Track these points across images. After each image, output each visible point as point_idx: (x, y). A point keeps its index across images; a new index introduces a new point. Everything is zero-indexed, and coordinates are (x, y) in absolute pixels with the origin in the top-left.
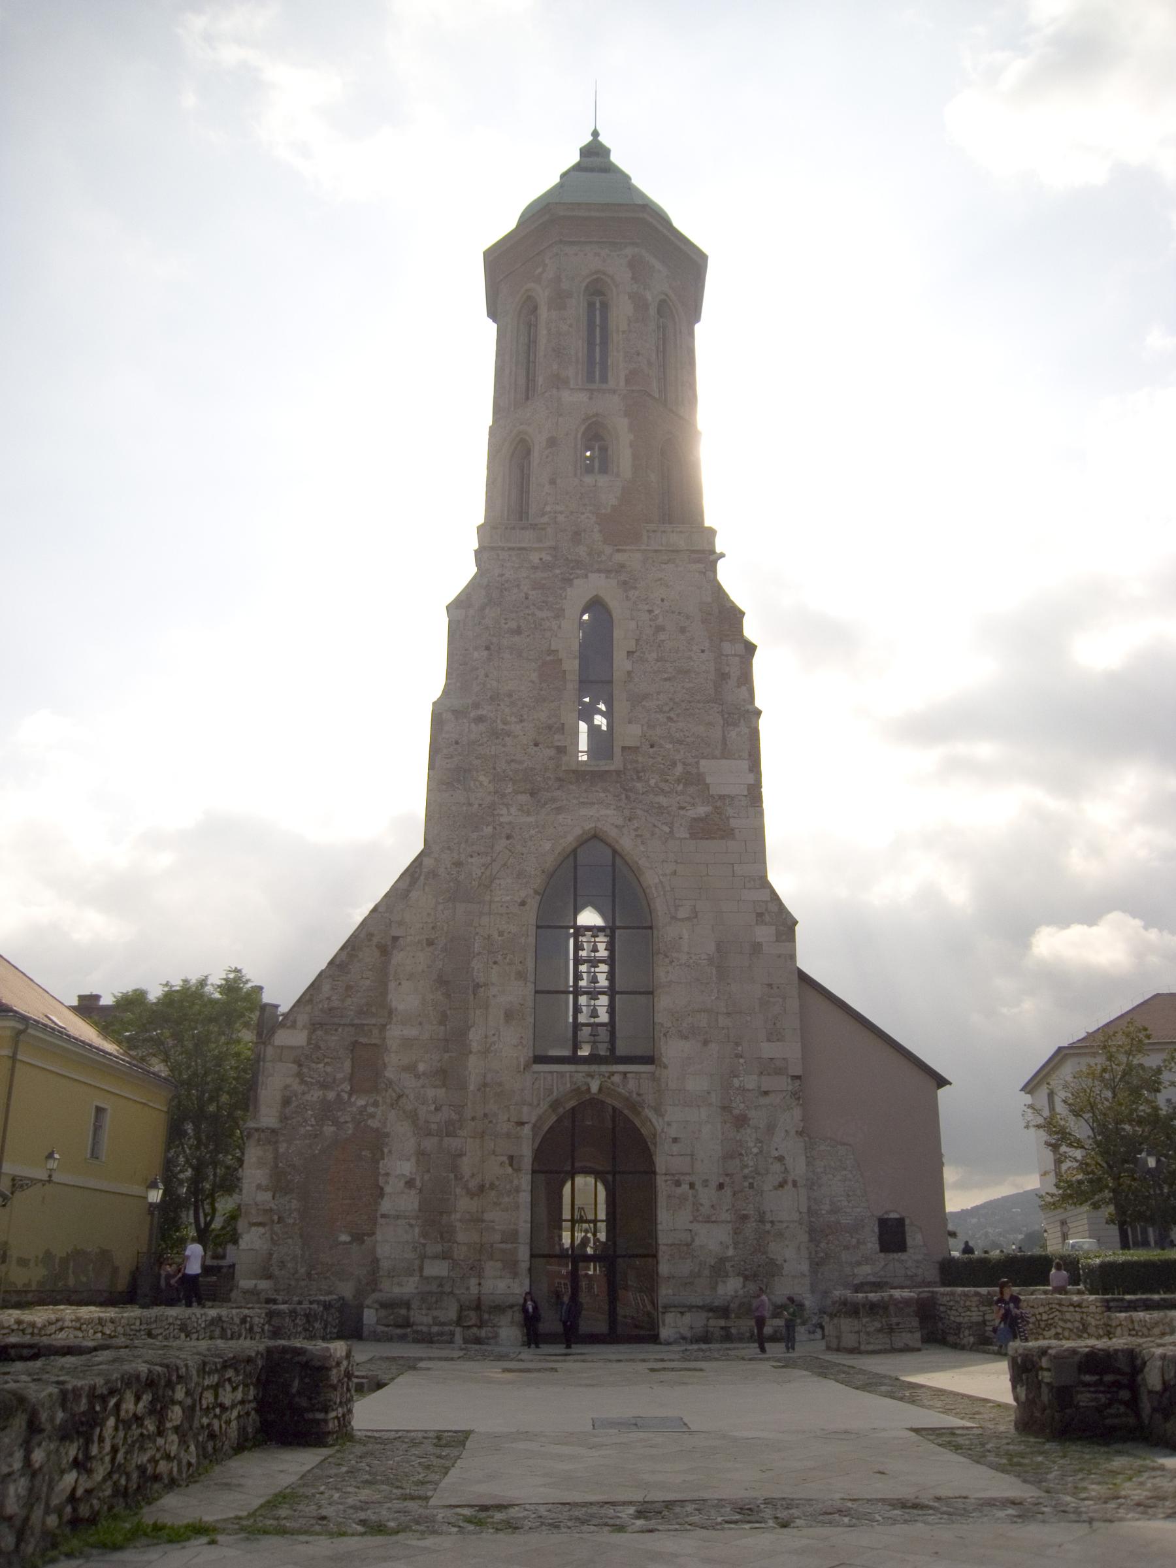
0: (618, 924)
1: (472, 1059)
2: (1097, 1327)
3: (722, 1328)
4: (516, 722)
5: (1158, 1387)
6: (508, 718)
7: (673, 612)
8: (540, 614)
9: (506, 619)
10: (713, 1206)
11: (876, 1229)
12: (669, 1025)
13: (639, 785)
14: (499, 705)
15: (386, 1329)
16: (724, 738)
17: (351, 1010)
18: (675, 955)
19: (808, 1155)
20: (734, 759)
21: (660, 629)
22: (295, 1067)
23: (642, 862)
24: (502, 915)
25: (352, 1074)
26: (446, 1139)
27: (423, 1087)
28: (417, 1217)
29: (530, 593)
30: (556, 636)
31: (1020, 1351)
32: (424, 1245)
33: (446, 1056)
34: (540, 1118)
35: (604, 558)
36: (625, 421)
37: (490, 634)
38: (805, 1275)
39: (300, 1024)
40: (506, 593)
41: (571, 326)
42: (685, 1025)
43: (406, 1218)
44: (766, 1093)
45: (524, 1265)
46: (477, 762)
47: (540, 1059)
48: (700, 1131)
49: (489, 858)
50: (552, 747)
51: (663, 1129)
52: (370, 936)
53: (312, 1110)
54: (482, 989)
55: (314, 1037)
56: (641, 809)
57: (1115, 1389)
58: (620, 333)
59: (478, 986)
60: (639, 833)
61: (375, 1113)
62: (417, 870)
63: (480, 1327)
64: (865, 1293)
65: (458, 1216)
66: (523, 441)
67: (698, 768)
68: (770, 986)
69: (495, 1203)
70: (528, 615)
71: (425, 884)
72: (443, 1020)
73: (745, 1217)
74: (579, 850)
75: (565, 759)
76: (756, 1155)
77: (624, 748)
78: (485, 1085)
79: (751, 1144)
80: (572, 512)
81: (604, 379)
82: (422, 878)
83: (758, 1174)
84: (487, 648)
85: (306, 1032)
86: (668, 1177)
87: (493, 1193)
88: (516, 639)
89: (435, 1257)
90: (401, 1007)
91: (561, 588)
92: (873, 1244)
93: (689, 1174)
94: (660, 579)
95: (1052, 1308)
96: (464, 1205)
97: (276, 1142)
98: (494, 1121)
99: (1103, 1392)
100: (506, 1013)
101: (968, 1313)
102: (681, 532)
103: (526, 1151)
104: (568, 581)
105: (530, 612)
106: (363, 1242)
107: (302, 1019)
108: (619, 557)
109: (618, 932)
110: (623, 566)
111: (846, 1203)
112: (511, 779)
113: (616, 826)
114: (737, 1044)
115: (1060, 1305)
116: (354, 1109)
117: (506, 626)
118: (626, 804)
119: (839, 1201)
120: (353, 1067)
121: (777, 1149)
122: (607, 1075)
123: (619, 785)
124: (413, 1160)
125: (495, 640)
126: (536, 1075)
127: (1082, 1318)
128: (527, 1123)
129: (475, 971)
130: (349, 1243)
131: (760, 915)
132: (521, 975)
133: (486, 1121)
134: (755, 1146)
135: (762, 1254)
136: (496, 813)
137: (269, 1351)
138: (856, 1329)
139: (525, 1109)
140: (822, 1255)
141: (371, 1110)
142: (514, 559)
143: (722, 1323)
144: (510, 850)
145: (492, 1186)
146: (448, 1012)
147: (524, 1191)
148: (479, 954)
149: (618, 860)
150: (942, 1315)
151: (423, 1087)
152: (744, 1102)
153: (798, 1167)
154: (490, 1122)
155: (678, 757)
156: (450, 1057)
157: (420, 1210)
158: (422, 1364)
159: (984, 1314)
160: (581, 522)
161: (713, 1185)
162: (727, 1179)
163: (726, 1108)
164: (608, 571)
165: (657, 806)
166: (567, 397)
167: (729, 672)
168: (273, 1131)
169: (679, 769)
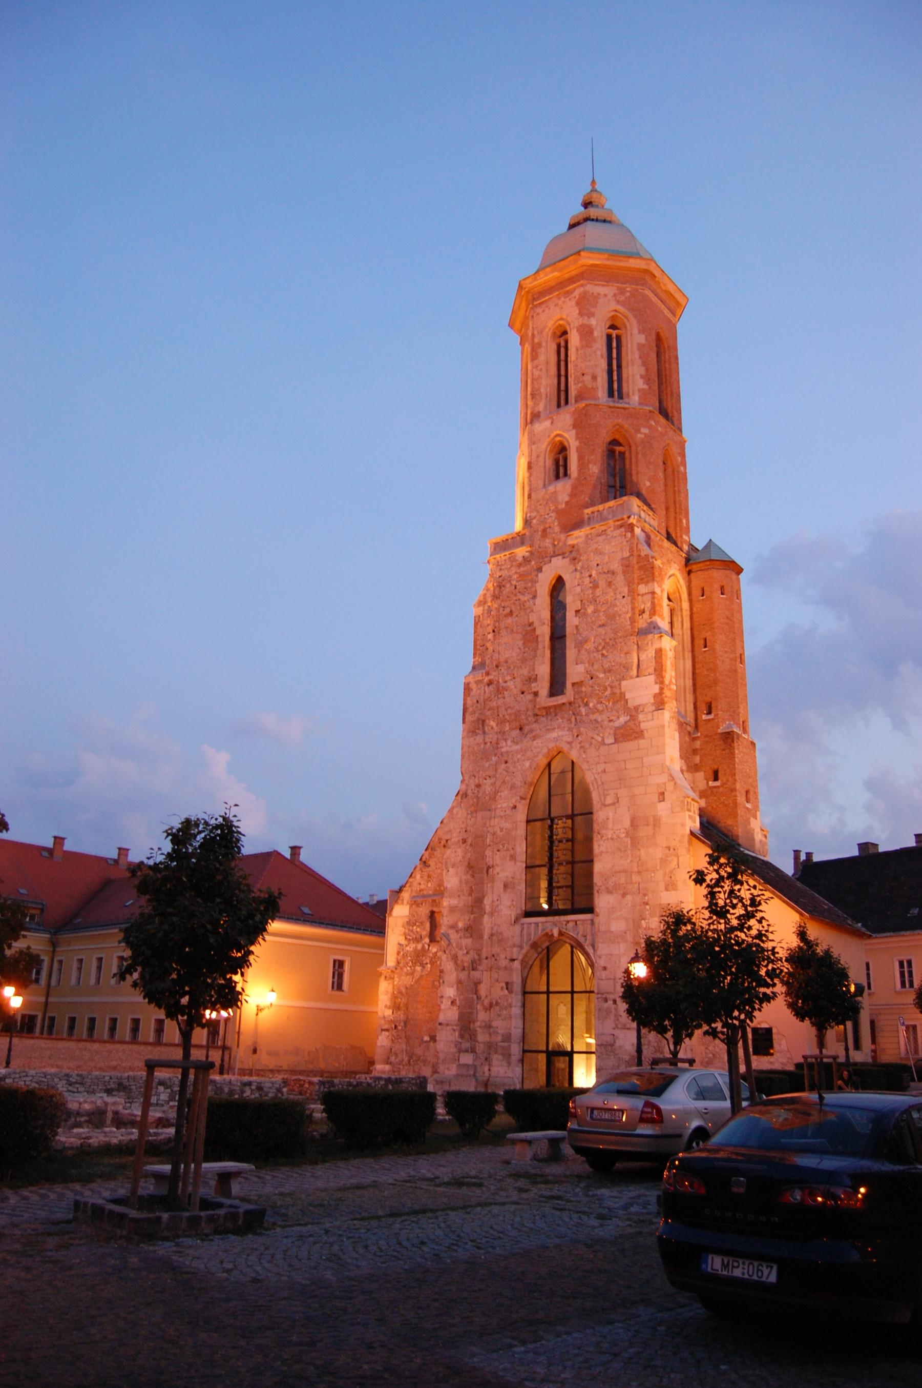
8: (524, 598)
23: (585, 766)
24: (501, 817)
26: (472, 972)
28: (457, 1025)
32: (461, 1043)
33: (472, 916)
34: (526, 955)
39: (405, 902)
41: (541, 370)
42: (610, 883)
46: (489, 713)
47: (528, 914)
48: (620, 962)
54: (491, 870)
60: (583, 744)
67: (620, 689)
75: (538, 699)
77: (573, 684)
78: (492, 935)
81: (567, 403)
85: (408, 906)
86: (599, 996)
87: (497, 1008)
88: (509, 620)
89: (467, 1051)
90: (449, 886)
96: (482, 1016)
104: (540, 569)
105: (517, 598)
108: (571, 542)
110: (573, 546)
113: (568, 743)
114: (645, 895)
116: (431, 955)
122: (564, 923)
124: (455, 987)
130: (430, 1041)
132: (513, 858)
133: (493, 959)
139: (515, 950)
140: (711, 1055)
145: (497, 1004)
147: (515, 1006)
148: (489, 845)
151: (460, 938)
154: (496, 960)
155: (607, 684)
164: (563, 555)
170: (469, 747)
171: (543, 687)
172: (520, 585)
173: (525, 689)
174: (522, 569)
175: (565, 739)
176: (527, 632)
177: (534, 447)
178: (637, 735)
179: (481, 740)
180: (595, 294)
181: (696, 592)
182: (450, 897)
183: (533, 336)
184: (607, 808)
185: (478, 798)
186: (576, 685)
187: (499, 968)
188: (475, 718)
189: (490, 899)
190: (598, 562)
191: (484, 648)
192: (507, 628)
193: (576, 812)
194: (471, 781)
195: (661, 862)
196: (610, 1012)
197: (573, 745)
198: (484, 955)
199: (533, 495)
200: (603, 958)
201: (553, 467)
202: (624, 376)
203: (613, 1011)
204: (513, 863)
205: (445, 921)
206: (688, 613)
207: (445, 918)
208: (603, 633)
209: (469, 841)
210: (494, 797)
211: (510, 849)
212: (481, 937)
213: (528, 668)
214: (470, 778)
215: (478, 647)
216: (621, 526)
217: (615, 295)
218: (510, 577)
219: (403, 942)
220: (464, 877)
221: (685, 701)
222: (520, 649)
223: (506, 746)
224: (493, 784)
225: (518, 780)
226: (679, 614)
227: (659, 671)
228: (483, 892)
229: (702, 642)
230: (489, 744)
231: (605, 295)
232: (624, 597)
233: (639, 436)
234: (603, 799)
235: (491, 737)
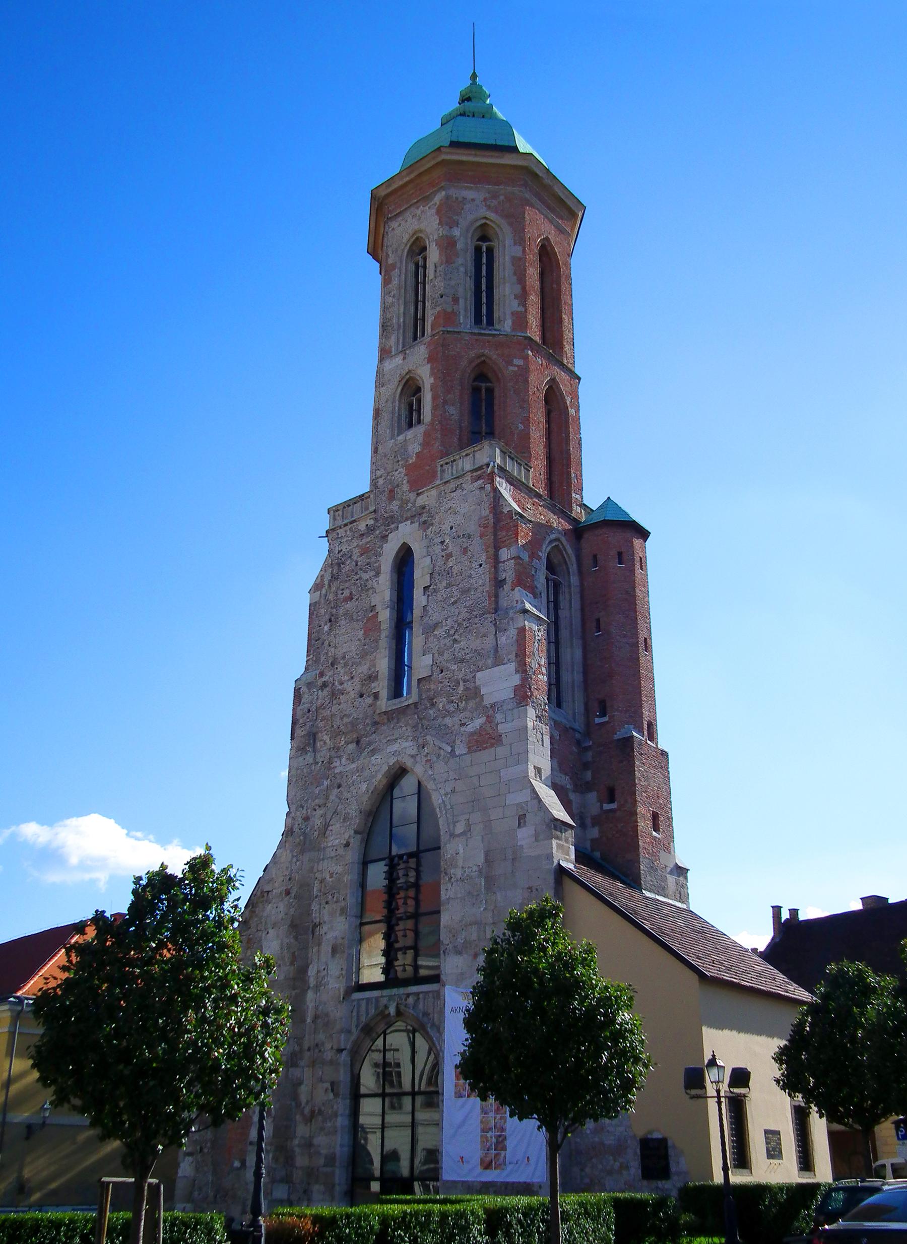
1: (310, 995)
4: (348, 680)
7: (459, 537)
8: (365, 576)
20: (504, 664)
24: (332, 858)
26: (291, 1070)
29: (359, 559)
33: (294, 993)
40: (342, 566)
41: (394, 296)
46: (321, 724)
60: (429, 758)
67: (475, 682)
68: (530, 888)
70: (357, 580)
75: (378, 703)
78: (316, 1017)
81: (423, 335)
84: (330, 621)
87: (320, 1118)
88: (349, 605)
92: (635, 1168)
96: (302, 1130)
98: (322, 1050)
100: (332, 948)
102: (467, 455)
104: (384, 538)
108: (421, 501)
110: (424, 507)
112: (344, 733)
122: (404, 997)
129: (314, 912)
132: (343, 911)
145: (320, 1112)
154: (320, 1051)
156: (296, 993)
170: (297, 769)
171: (382, 687)
172: (362, 561)
173: (364, 690)
177: (382, 390)
178: (493, 741)
179: (311, 761)
180: (460, 199)
181: (587, 561)
185: (304, 834)
186: (423, 682)
189: (316, 968)
190: (451, 524)
191: (320, 642)
193: (422, 848)
197: (418, 759)
199: (380, 448)
201: (404, 413)
202: (496, 297)
204: (343, 918)
206: (578, 590)
212: (304, 1021)
214: (297, 810)
215: (313, 642)
216: (479, 478)
217: (485, 200)
218: (351, 551)
221: (574, 701)
222: (359, 640)
224: (323, 816)
225: (353, 810)
226: (567, 590)
227: (521, 656)
229: (594, 624)
231: (473, 200)
232: (481, 565)
233: (511, 368)
235: (323, 754)
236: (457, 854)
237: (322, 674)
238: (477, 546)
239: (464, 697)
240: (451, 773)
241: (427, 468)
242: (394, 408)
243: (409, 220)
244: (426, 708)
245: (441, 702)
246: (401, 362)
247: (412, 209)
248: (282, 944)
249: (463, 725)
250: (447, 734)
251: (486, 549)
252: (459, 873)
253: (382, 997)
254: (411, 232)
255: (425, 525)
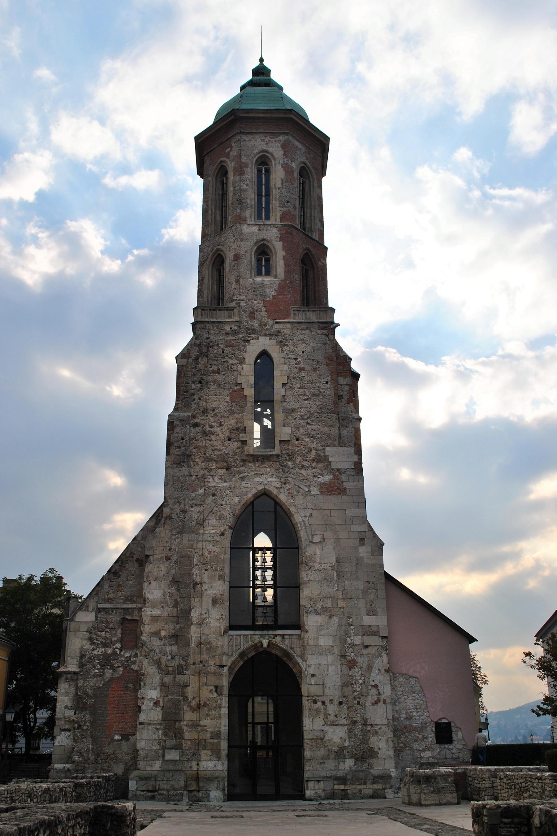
0: (278, 546)
1: (193, 629)
2: (550, 791)
3: (343, 790)
5: (538, 825)
6: (213, 424)
8: (231, 361)
9: (211, 365)
10: (336, 716)
11: (434, 729)
12: (309, 606)
13: (289, 463)
14: (207, 416)
15: (142, 793)
16: (340, 434)
17: (122, 599)
18: (312, 564)
19: (392, 684)
21: (301, 370)
22: (88, 635)
23: (292, 509)
24: (210, 541)
25: (122, 638)
26: (178, 676)
27: (164, 645)
28: (161, 724)
29: (225, 349)
30: (240, 374)
31: (475, 806)
32: (165, 741)
33: (178, 626)
34: (233, 663)
35: (268, 327)
36: (281, 243)
37: (201, 374)
38: (391, 758)
39: (90, 608)
40: (211, 349)
41: (247, 185)
42: (317, 606)
43: (154, 724)
44: (367, 647)
45: (224, 753)
46: (195, 450)
47: (232, 627)
49: (202, 508)
50: (238, 441)
51: (306, 669)
52: (132, 554)
53: (98, 660)
55: (99, 616)
56: (292, 477)
57: (519, 826)
58: (277, 189)
59: (196, 584)
61: (136, 661)
62: (160, 515)
63: (198, 791)
64: (425, 769)
65: (185, 723)
66: (220, 255)
67: (325, 453)
69: (207, 715)
70: (224, 362)
71: (164, 524)
72: (176, 604)
73: (355, 722)
74: (255, 502)
75: (246, 448)
76: (361, 684)
77: (281, 441)
78: (201, 644)
79: (359, 678)
80: (249, 300)
81: (268, 218)
82: (163, 520)
83: (363, 696)
84: (200, 382)
85: (94, 613)
86: (310, 698)
87: (206, 709)
88: (217, 376)
89: (172, 748)
90: (151, 597)
91: (243, 346)
92: (431, 738)
93: (322, 696)
94: (302, 340)
95: (527, 780)
96: (189, 716)
97: (77, 679)
99: (513, 828)
100: (212, 600)
101: (484, 782)
102: (313, 311)
103: (225, 683)
104: (248, 341)
105: (225, 360)
106: (129, 740)
107: (92, 604)
108: (276, 327)
109: (278, 550)
110: (280, 332)
111: (415, 714)
112: (215, 460)
113: (277, 488)
115: (531, 778)
117: (211, 369)
118: (282, 475)
119: (411, 712)
120: (122, 634)
121: (373, 681)
122: (273, 636)
123: (278, 463)
124: (158, 689)
125: (204, 377)
126: (231, 637)
127: (542, 786)
128: (226, 666)
131: (362, 540)
132: (221, 577)
134: (360, 679)
135: (366, 745)
136: (206, 480)
137: (95, 807)
138: (419, 791)
139: (224, 657)
141: (133, 659)
142: (215, 328)
143: (342, 787)
144: (215, 503)
145: (205, 705)
146: (179, 600)
147: (224, 707)
148: (197, 565)
149: (278, 508)
150: (470, 783)
151: (164, 645)
152: (353, 653)
153: (387, 691)
154: (204, 666)
157: (162, 720)
158: (165, 814)
159: (493, 783)
160: (254, 306)
161: (336, 702)
162: (344, 699)
163: (343, 656)
164: (270, 335)
165: (300, 475)
166: (245, 229)
167: (342, 395)
168: (75, 673)
169: (314, 453)
173: (232, 436)
174: (230, 337)
175: (273, 484)
176: (234, 391)
177: (242, 243)
182: (153, 607)
183: (239, 156)
184: (314, 545)
185: (183, 522)
186: (283, 444)
187: (208, 673)
188: (180, 453)
191: (188, 394)
192: (214, 382)
194: (176, 507)
195: (363, 593)
196: (320, 711)
197: (282, 490)
198: (191, 661)
199: (241, 281)
200: (313, 667)
203: (322, 710)
204: (221, 582)
205: (147, 628)
207: (146, 626)
208: (309, 407)
209: (174, 558)
210: (201, 523)
211: (219, 569)
212: (188, 645)
213: (235, 420)
215: (182, 392)
216: (324, 328)
219: (87, 646)
220: (168, 591)
222: (227, 402)
223: (214, 482)
225: (227, 513)
228: (190, 605)
230: (194, 477)
233: (320, 263)
234: (310, 538)
236: (315, 554)
237: (194, 417)
238: (323, 369)
239: (316, 460)
240: (308, 504)
241: (282, 308)
242: (251, 259)
243: (259, 141)
244: (286, 460)
245: (299, 459)
246: (257, 231)
247: (261, 135)
248: (164, 592)
249: (316, 476)
250: (304, 480)
251: (331, 374)
252: (317, 566)
253: (254, 635)
254: (260, 148)
255: (281, 343)
